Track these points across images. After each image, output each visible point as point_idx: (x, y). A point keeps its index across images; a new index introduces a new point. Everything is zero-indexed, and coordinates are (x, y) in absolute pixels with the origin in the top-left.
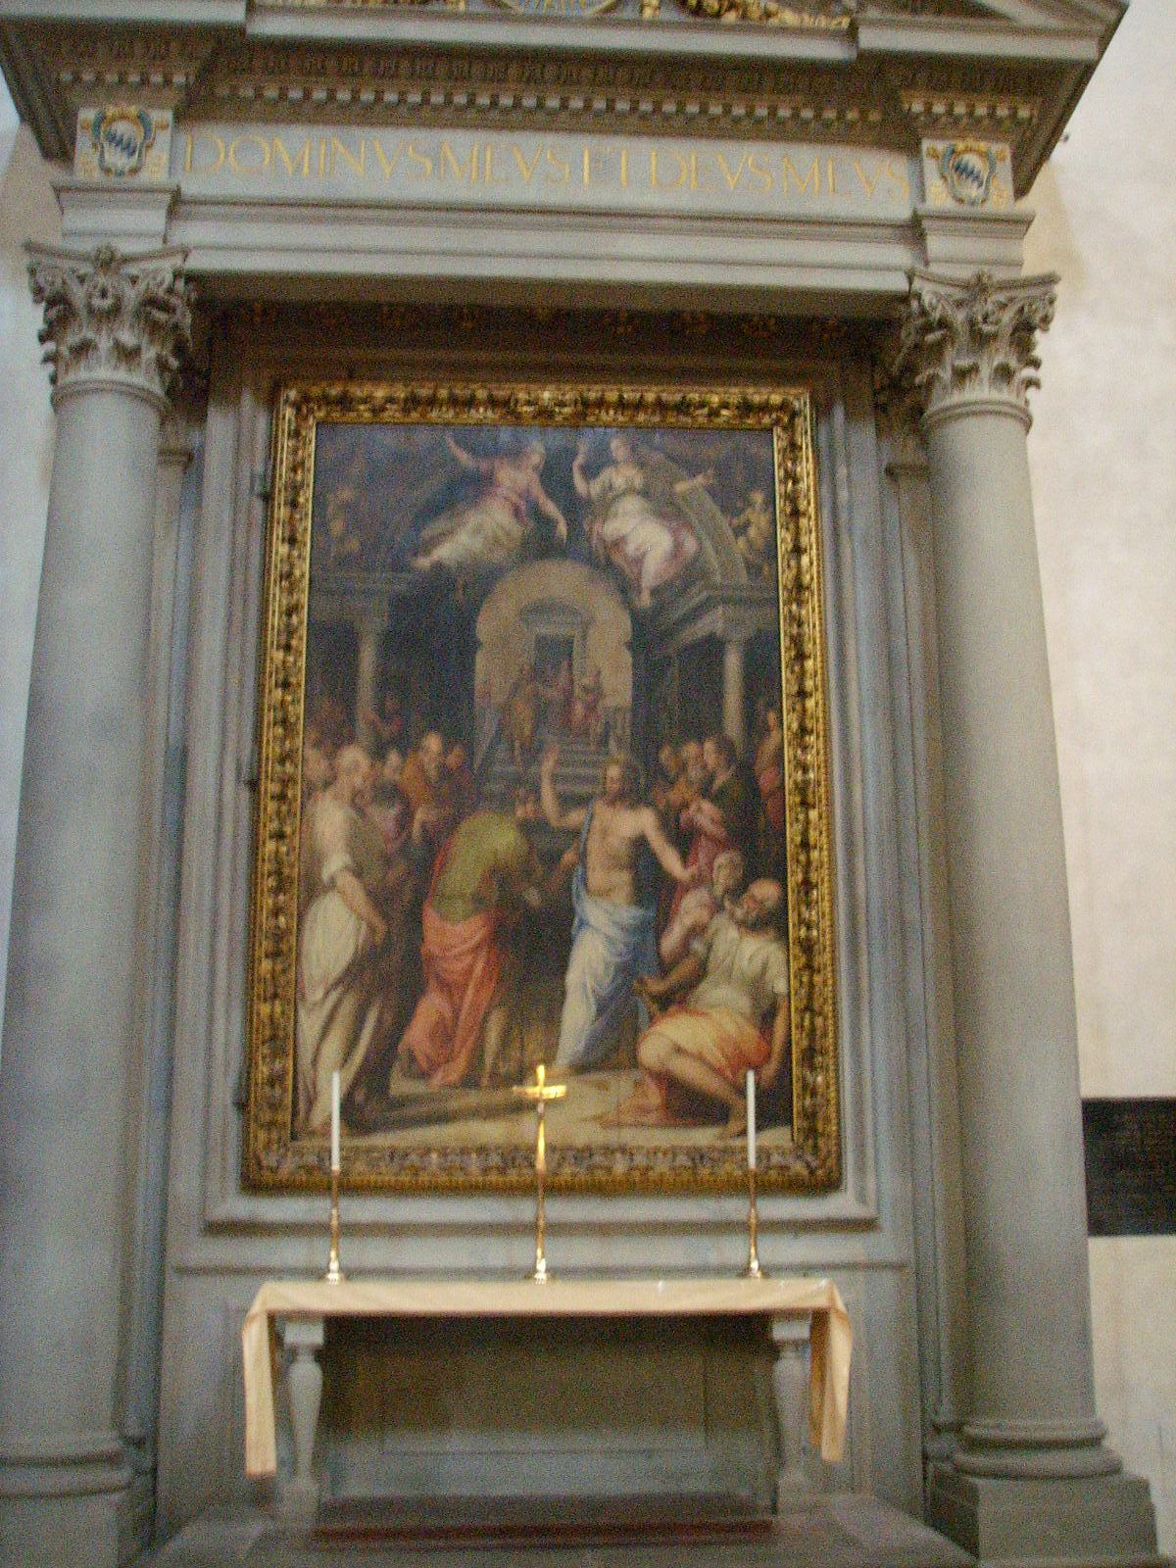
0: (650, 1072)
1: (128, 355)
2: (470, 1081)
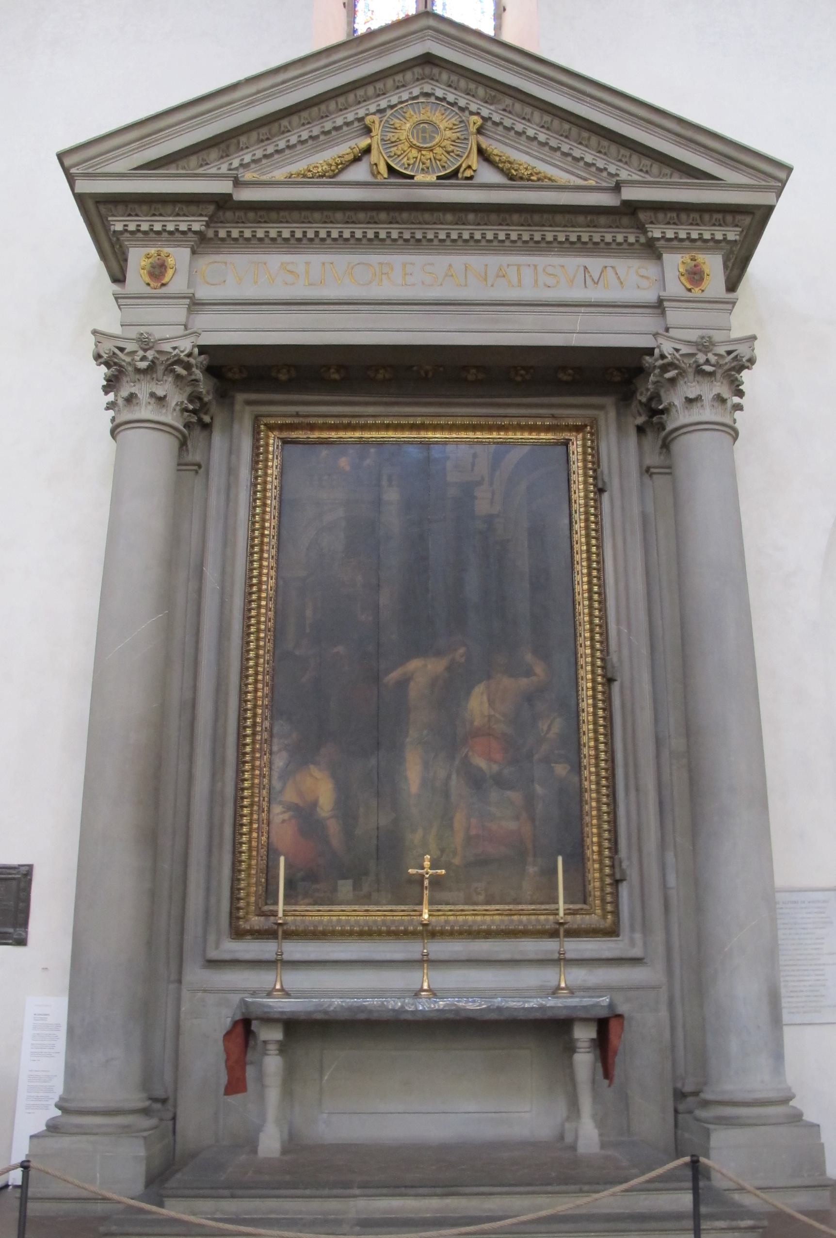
1: (161, 400)
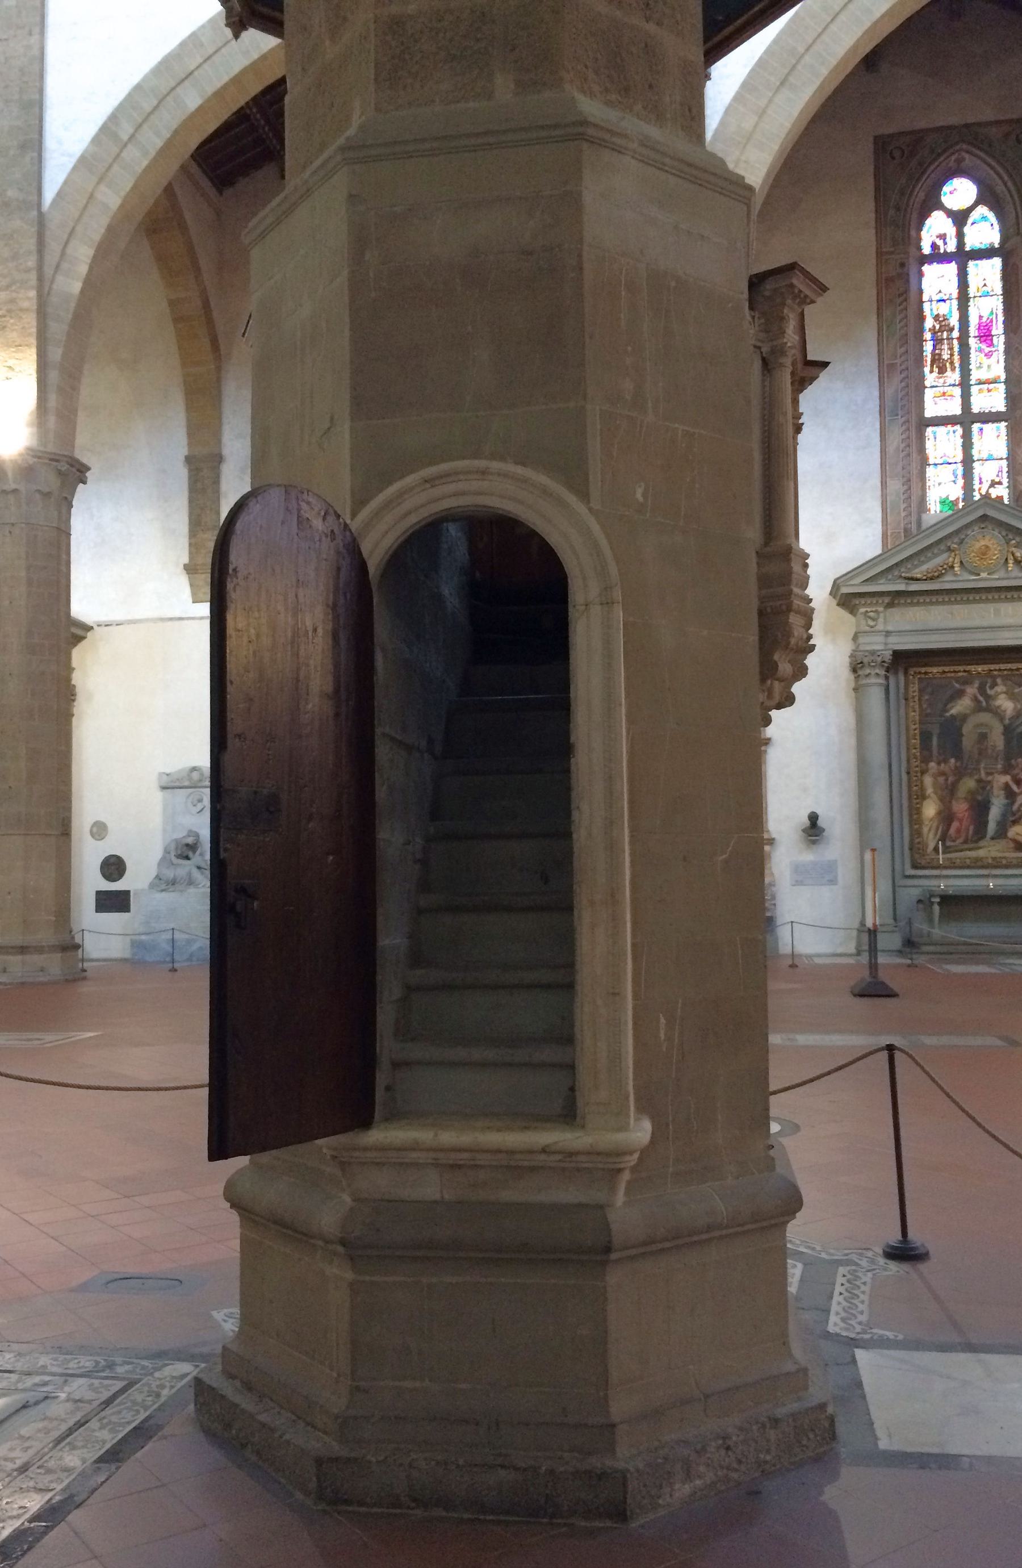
0: (1011, 839)
2: (965, 842)
